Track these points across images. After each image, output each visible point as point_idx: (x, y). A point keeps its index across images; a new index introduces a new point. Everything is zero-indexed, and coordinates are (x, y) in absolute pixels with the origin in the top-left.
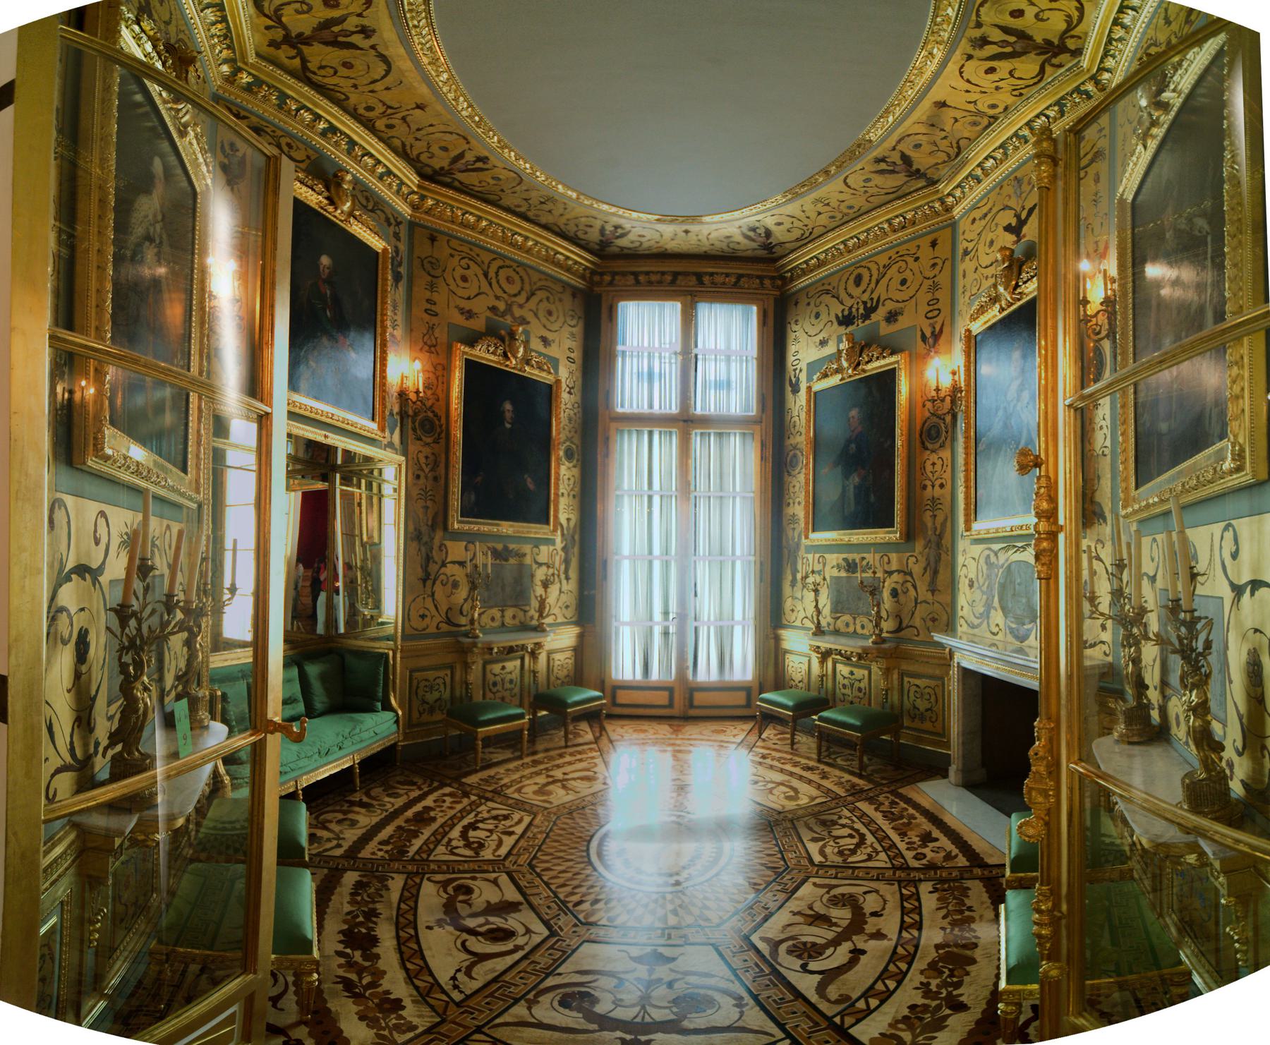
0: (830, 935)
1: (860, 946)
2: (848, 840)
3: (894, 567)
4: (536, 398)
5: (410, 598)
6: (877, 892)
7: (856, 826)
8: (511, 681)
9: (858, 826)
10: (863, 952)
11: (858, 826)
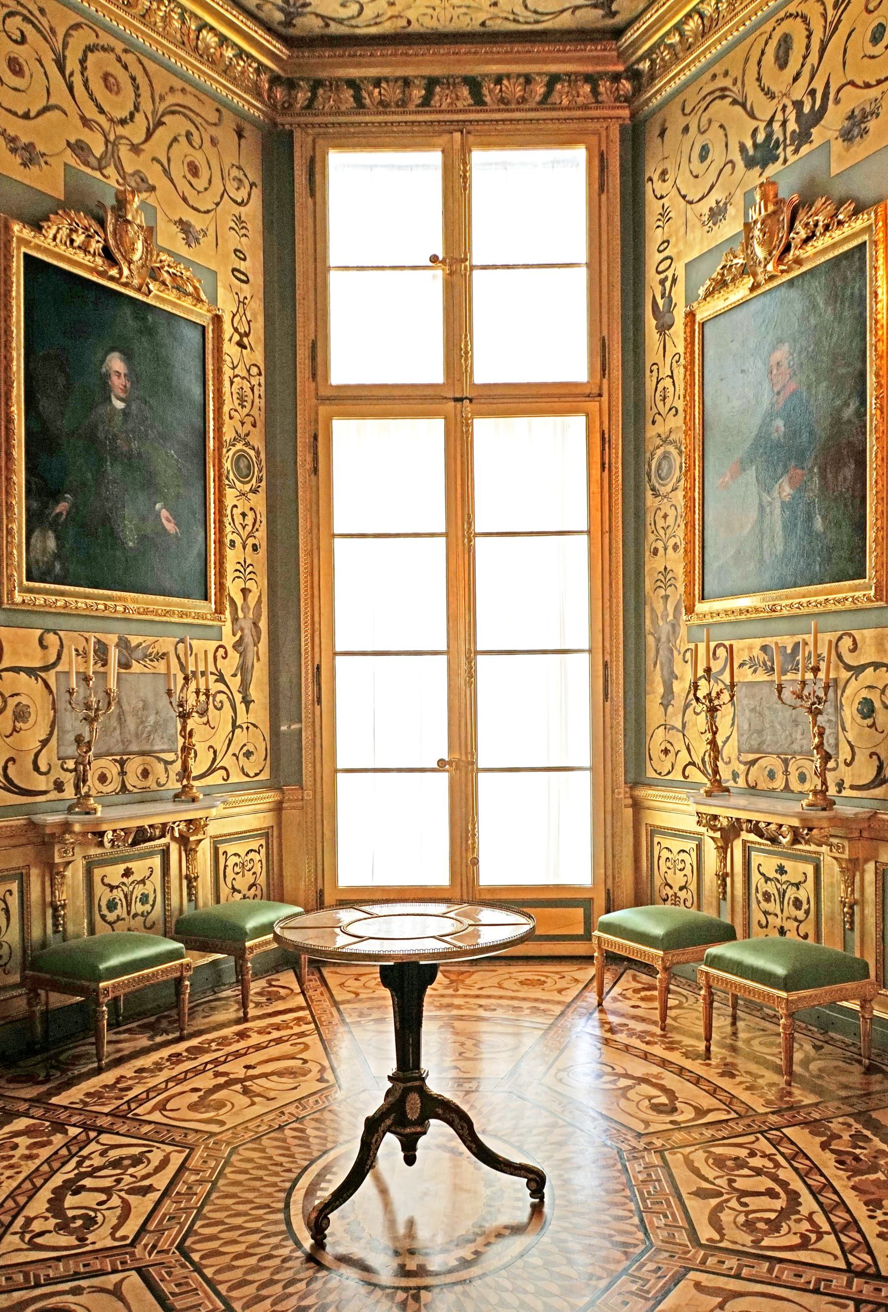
2: (765, 1202)
3: (867, 655)
7: (782, 1174)
9: (786, 1174)
11: (786, 1174)
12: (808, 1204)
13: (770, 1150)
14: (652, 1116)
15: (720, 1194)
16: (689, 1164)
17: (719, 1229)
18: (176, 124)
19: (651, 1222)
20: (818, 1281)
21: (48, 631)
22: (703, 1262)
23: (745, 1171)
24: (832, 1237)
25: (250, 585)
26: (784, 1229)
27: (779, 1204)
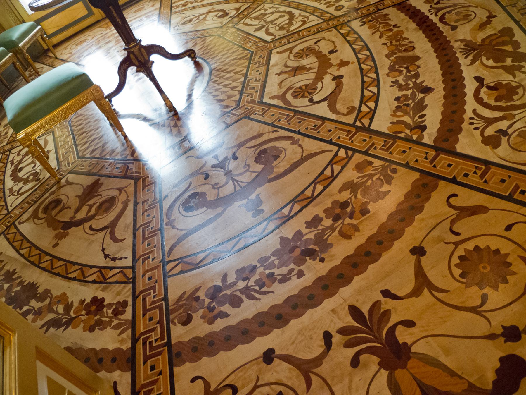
0: (313, 76)
1: (337, 74)
2: (281, 19)
6: (324, 39)
10: (341, 77)
11: (282, 8)
12: (296, 12)
13: (271, 6)
14: (221, 20)
15: (265, 26)
16: (246, 24)
17: (272, 35)
19: (248, 47)
20: (317, 29)
22: (274, 46)
23: (267, 16)
24: (312, 16)
26: (294, 23)
27: (287, 17)
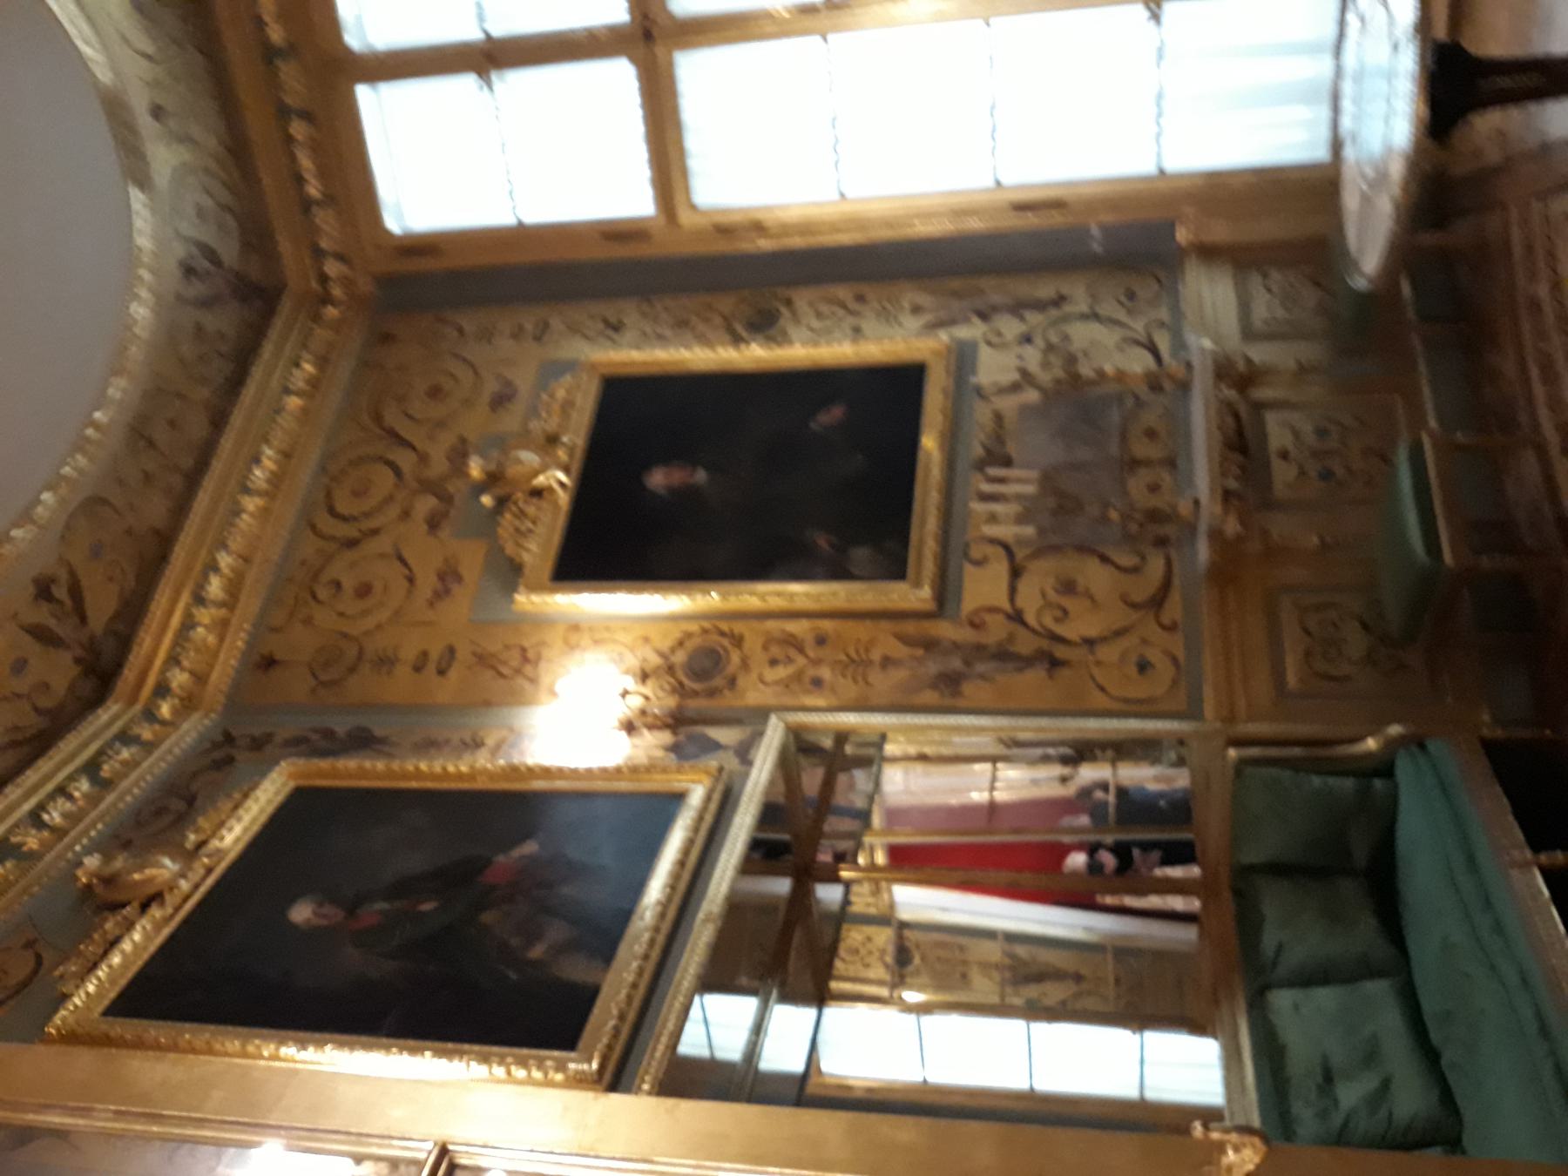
4: (635, 419)
5: (1100, 701)
8: (1322, 433)
18: (392, 418)
21: (966, 555)
25: (906, 305)
